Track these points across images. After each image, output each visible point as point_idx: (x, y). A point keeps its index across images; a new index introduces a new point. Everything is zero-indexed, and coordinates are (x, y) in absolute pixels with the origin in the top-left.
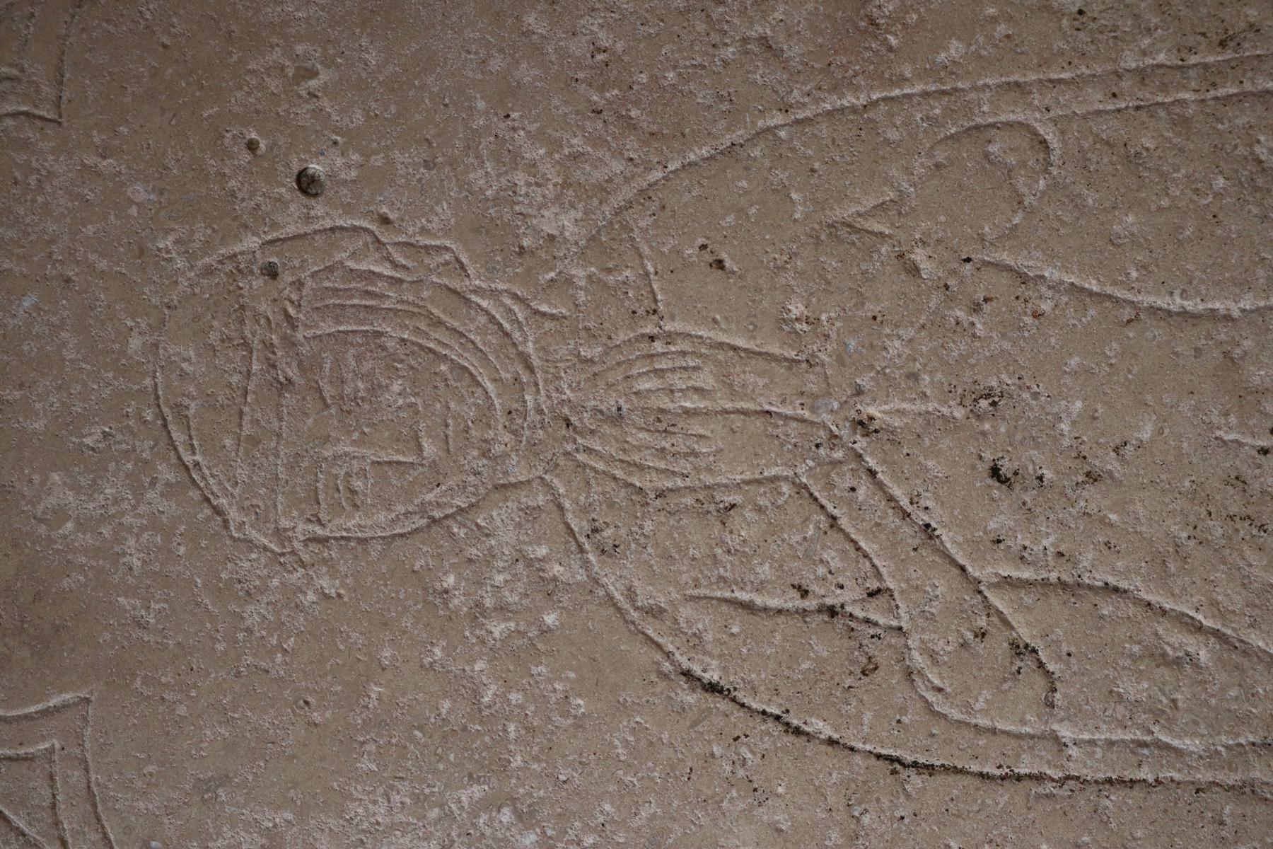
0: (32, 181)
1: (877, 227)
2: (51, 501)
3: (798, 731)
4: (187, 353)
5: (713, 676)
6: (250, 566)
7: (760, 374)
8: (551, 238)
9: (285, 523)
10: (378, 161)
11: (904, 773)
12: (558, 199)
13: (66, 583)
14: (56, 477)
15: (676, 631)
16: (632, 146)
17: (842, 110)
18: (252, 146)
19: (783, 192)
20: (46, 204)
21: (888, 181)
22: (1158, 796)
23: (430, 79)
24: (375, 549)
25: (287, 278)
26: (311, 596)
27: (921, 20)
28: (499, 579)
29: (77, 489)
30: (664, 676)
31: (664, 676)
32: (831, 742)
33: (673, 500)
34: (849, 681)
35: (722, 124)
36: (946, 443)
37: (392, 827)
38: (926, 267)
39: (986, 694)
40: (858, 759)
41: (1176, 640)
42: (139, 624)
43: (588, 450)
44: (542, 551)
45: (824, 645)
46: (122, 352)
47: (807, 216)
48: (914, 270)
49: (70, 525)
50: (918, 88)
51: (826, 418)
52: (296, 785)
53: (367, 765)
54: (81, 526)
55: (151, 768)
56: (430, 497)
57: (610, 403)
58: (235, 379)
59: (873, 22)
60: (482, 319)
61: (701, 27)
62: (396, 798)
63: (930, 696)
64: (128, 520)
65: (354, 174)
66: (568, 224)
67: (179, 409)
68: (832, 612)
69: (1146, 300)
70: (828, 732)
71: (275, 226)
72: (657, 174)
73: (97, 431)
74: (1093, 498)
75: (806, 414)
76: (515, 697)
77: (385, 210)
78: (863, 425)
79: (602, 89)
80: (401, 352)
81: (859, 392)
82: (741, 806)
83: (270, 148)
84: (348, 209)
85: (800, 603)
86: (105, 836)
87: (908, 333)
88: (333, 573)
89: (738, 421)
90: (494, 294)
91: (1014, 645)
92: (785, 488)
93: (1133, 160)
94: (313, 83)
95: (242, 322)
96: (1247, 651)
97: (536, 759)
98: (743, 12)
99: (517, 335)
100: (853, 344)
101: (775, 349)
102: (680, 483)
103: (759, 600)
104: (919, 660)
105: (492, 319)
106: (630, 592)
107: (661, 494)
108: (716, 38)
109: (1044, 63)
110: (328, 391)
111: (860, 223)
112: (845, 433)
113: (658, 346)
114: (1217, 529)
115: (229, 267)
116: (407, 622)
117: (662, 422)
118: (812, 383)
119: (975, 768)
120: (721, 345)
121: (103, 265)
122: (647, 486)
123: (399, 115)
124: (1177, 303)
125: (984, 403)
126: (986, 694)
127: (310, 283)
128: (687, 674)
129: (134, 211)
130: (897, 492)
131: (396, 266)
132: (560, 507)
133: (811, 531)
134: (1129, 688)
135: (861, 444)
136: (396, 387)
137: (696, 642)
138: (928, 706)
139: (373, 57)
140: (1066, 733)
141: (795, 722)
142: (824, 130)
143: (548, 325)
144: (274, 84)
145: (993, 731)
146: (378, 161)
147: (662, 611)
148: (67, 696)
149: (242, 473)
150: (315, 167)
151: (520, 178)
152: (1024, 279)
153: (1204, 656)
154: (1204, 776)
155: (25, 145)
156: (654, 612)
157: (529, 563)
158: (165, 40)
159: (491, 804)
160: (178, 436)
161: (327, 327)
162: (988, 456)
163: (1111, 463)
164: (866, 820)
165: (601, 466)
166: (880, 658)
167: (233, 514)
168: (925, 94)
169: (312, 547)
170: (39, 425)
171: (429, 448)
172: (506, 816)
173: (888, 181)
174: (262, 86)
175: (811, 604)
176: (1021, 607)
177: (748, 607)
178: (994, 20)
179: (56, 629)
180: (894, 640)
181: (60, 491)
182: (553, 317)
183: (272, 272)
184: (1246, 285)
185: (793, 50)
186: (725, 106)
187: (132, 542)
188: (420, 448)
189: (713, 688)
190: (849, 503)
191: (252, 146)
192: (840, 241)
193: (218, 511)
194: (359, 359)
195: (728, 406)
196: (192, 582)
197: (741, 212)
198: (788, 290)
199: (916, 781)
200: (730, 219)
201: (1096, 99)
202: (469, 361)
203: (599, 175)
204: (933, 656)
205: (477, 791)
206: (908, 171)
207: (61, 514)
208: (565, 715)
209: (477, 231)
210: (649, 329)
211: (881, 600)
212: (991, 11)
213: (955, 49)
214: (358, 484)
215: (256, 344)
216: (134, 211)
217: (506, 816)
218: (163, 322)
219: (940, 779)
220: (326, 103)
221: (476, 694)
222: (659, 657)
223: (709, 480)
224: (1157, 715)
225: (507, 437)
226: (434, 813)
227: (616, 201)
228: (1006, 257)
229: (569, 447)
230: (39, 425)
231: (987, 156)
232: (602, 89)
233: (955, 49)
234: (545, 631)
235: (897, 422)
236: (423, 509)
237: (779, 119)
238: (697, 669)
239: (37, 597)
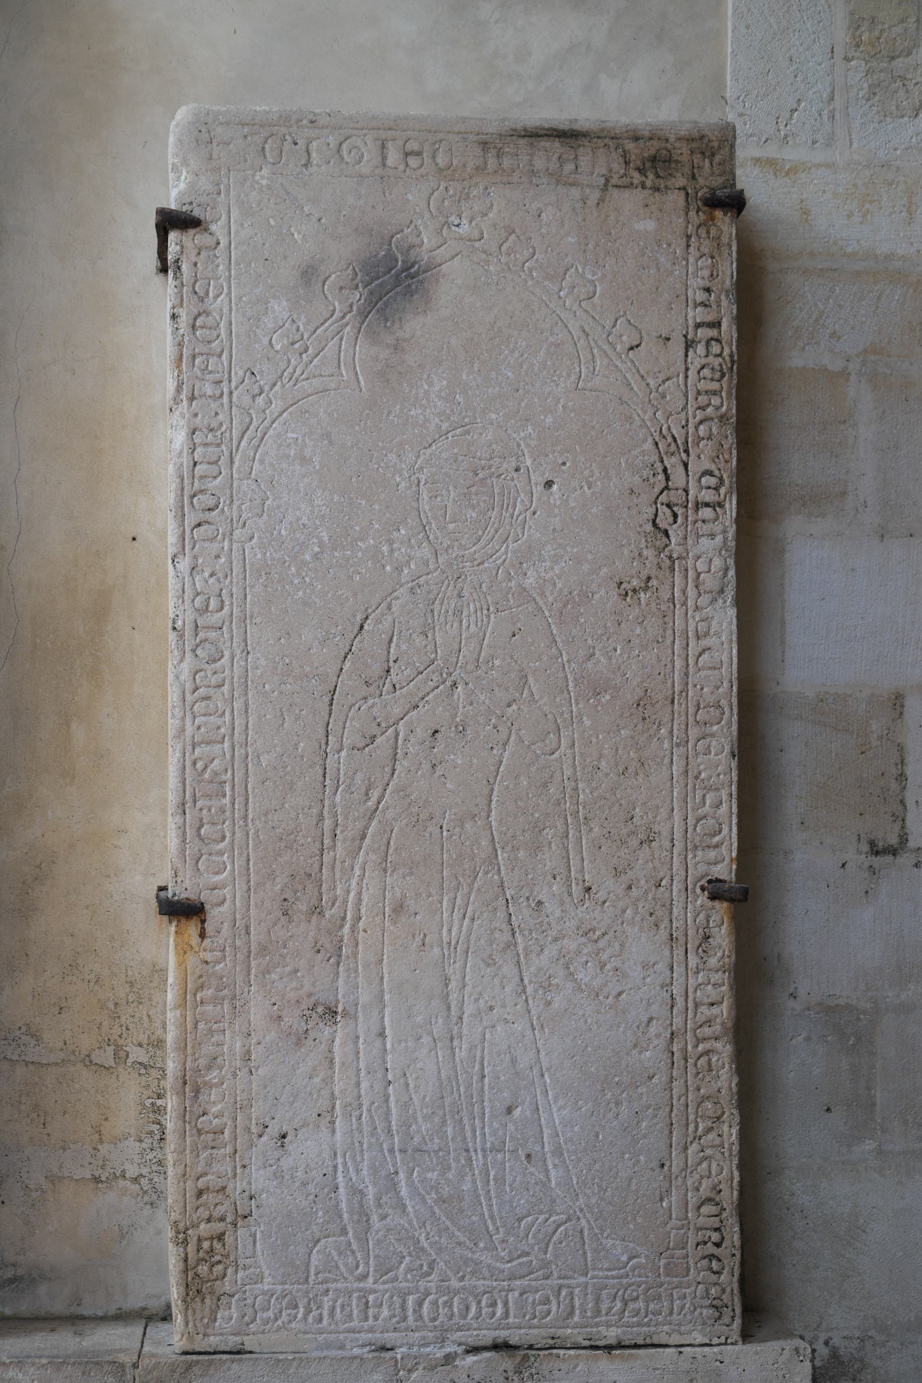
0: (556, 378)
1: (525, 692)
2: (436, 381)
3: (345, 657)
4: (489, 436)
5: (366, 627)
6: (410, 456)
7: (474, 649)
8: (526, 574)
9: (425, 471)
10: (557, 511)
11: (330, 695)
12: (540, 577)
13: (405, 385)
14: (445, 382)
15: (383, 615)
16: (558, 605)
17: (567, 682)
18: (564, 464)
19: (539, 659)
20: (546, 383)
21: (542, 697)
22: (320, 786)
23: (585, 532)
24: (415, 504)
25: (515, 475)
26: (398, 479)
27: (598, 711)
28: (403, 550)
29: (440, 391)
30: (366, 610)
31: (366, 610)
32: (341, 669)
33: (429, 615)
34: (363, 676)
35: (564, 638)
36: (447, 714)
37: (313, 506)
38: (510, 710)
39: (358, 726)
40: (335, 678)
41: (375, 794)
42: (389, 413)
43: (449, 584)
44: (413, 566)
45: (377, 669)
46: (490, 411)
47: (530, 667)
48: (509, 705)
49: (426, 387)
50: (574, 710)
51: (458, 671)
52: (329, 470)
53: (336, 498)
54: (426, 392)
55: (335, 415)
56: (434, 526)
57: (465, 593)
58: (479, 454)
59: (598, 694)
60: (497, 548)
61: (599, 632)
62: (324, 508)
63: (357, 706)
64: (428, 410)
65: (552, 502)
66: (530, 581)
67: (467, 432)
68: (388, 671)
69: (496, 788)
70: (345, 669)
71: (535, 471)
72: (547, 614)
73: (461, 400)
74: (426, 766)
75: (459, 665)
76: (360, 554)
77: (538, 513)
78: (454, 685)
79: (579, 595)
80: (487, 517)
81: (466, 684)
82: (319, 636)
83: (563, 471)
84: (539, 499)
85: (391, 660)
86: (310, 395)
87: (487, 702)
88: (407, 488)
89: (457, 640)
90: (506, 553)
91: (375, 736)
92: (433, 656)
93: (545, 785)
94: (586, 488)
95: (500, 457)
96: (371, 819)
97: (337, 561)
98: (604, 648)
99: (491, 560)
100: (484, 682)
101: (483, 654)
102: (436, 618)
103: (393, 645)
104: (370, 702)
105: (497, 551)
106: (397, 598)
107: (432, 611)
108: (595, 637)
109: (581, 755)
110: (473, 489)
111: (527, 686)
112: (452, 678)
113: (485, 612)
114: (415, 810)
115: (520, 453)
116: (388, 515)
117: (458, 612)
118: (471, 667)
119: (331, 721)
120: (485, 635)
121: (523, 404)
122: (435, 606)
123: (572, 519)
124: (494, 798)
125: (461, 728)
126: (358, 726)
127: (513, 484)
128: (367, 618)
129: (542, 417)
130: (430, 696)
131: (518, 516)
132: (428, 574)
133: (417, 664)
134: (359, 777)
135: (448, 683)
136: (474, 515)
137: (378, 622)
138: (354, 705)
139: (594, 510)
140: (343, 754)
141: (349, 656)
142: (561, 675)
143: (494, 572)
144: (586, 473)
145: (344, 728)
146: (557, 511)
147: (390, 609)
148: (362, 383)
149: (444, 455)
150: (555, 487)
151: (548, 564)
152: (505, 744)
153: (370, 803)
154: (327, 803)
155: (569, 376)
156: (389, 607)
157: (408, 562)
158: (605, 432)
159: (321, 544)
160: (458, 431)
161: (496, 490)
162: (442, 729)
163: (438, 773)
164: (313, 681)
165: (443, 589)
166: (371, 688)
167: (429, 451)
168: (572, 712)
169: (416, 481)
170: (464, 377)
171: (451, 526)
172: (317, 549)
173: (542, 697)
174: (586, 468)
175: (391, 664)
176: (388, 740)
177: (391, 641)
178: (598, 737)
179: (388, 380)
180: (378, 693)
181: (439, 384)
182: (497, 574)
183: (517, 470)
184: (500, 822)
185: (590, 665)
186: (570, 640)
187: (420, 411)
188: (451, 523)
189: (362, 627)
190: (427, 679)
191: (564, 464)
192: (521, 679)
193: (430, 445)
194: (485, 501)
195: (463, 637)
196: (405, 434)
197: (532, 644)
198: (504, 660)
199: (327, 699)
200: (530, 640)
201: (568, 772)
202: (483, 542)
203: (548, 593)
204: (372, 707)
205: (326, 539)
206: (545, 704)
207: (431, 384)
208: (353, 572)
209: (529, 547)
210: (491, 609)
211: (392, 689)
212: (601, 737)
213: (588, 723)
214: (439, 499)
215: (492, 462)
216: (542, 417)
217: (317, 549)
218: (501, 427)
219: (328, 708)
220: (578, 492)
221: (362, 540)
222: (374, 608)
223: (437, 629)
224: (349, 787)
225: (454, 555)
226: (318, 523)
227: (538, 599)
228: (513, 738)
229: (450, 578)
230: (464, 377)
231: (549, 733)
232: (579, 595)
233: (588, 723)
234: (384, 566)
235: (455, 697)
236: (429, 523)
237: (565, 659)
238: (368, 621)
239: (400, 373)
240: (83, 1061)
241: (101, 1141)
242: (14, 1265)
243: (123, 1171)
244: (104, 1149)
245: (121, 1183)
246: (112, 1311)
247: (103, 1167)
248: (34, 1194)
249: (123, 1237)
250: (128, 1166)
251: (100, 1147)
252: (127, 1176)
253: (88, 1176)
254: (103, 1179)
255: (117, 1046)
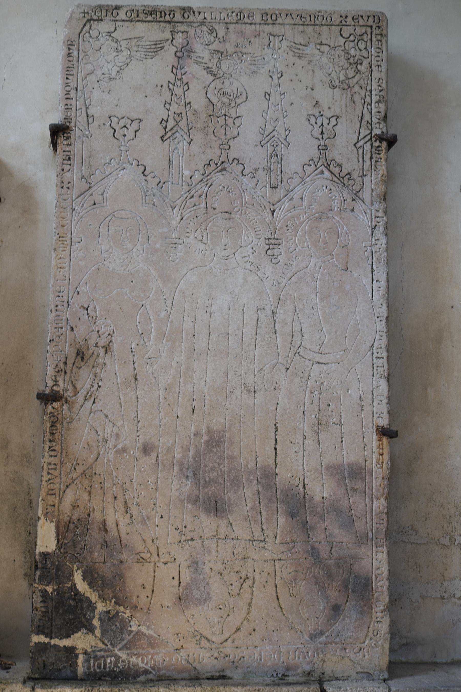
240: (436, 543)
241: (444, 580)
242: (406, 638)
243: (454, 595)
244: (446, 584)
245: (453, 600)
246: (449, 660)
247: (445, 592)
248: (415, 604)
249: (454, 625)
250: (456, 592)
251: (444, 583)
252: (456, 596)
253: (439, 596)
254: (445, 597)
255: (451, 536)
